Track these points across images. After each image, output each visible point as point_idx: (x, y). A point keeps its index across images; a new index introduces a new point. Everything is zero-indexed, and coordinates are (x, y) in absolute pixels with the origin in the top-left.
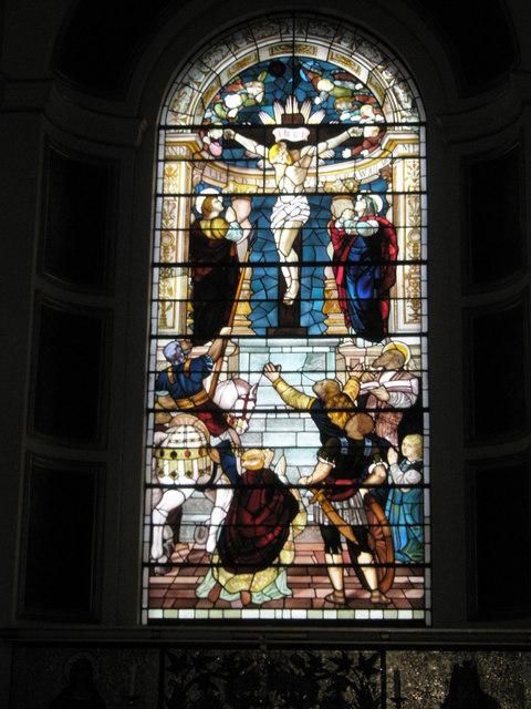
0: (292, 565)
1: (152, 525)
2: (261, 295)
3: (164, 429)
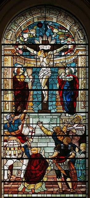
0: (47, 181)
1: (4, 170)
2: (36, 100)
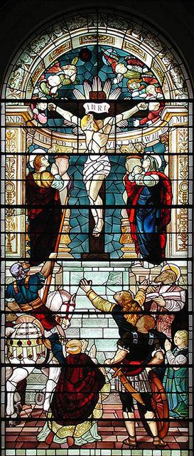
0: (101, 419)
1: (6, 392)
2: (77, 230)
3: (12, 326)
